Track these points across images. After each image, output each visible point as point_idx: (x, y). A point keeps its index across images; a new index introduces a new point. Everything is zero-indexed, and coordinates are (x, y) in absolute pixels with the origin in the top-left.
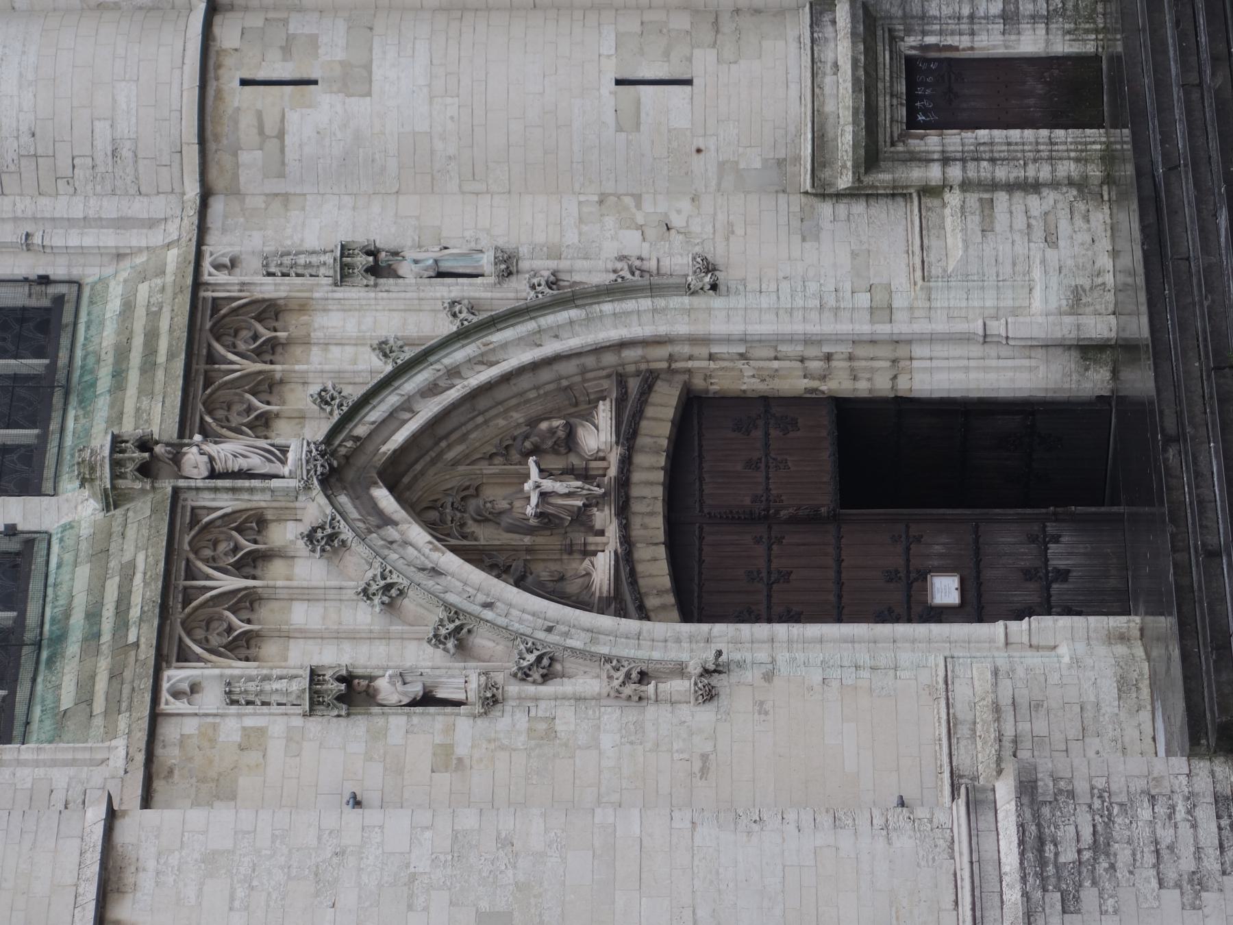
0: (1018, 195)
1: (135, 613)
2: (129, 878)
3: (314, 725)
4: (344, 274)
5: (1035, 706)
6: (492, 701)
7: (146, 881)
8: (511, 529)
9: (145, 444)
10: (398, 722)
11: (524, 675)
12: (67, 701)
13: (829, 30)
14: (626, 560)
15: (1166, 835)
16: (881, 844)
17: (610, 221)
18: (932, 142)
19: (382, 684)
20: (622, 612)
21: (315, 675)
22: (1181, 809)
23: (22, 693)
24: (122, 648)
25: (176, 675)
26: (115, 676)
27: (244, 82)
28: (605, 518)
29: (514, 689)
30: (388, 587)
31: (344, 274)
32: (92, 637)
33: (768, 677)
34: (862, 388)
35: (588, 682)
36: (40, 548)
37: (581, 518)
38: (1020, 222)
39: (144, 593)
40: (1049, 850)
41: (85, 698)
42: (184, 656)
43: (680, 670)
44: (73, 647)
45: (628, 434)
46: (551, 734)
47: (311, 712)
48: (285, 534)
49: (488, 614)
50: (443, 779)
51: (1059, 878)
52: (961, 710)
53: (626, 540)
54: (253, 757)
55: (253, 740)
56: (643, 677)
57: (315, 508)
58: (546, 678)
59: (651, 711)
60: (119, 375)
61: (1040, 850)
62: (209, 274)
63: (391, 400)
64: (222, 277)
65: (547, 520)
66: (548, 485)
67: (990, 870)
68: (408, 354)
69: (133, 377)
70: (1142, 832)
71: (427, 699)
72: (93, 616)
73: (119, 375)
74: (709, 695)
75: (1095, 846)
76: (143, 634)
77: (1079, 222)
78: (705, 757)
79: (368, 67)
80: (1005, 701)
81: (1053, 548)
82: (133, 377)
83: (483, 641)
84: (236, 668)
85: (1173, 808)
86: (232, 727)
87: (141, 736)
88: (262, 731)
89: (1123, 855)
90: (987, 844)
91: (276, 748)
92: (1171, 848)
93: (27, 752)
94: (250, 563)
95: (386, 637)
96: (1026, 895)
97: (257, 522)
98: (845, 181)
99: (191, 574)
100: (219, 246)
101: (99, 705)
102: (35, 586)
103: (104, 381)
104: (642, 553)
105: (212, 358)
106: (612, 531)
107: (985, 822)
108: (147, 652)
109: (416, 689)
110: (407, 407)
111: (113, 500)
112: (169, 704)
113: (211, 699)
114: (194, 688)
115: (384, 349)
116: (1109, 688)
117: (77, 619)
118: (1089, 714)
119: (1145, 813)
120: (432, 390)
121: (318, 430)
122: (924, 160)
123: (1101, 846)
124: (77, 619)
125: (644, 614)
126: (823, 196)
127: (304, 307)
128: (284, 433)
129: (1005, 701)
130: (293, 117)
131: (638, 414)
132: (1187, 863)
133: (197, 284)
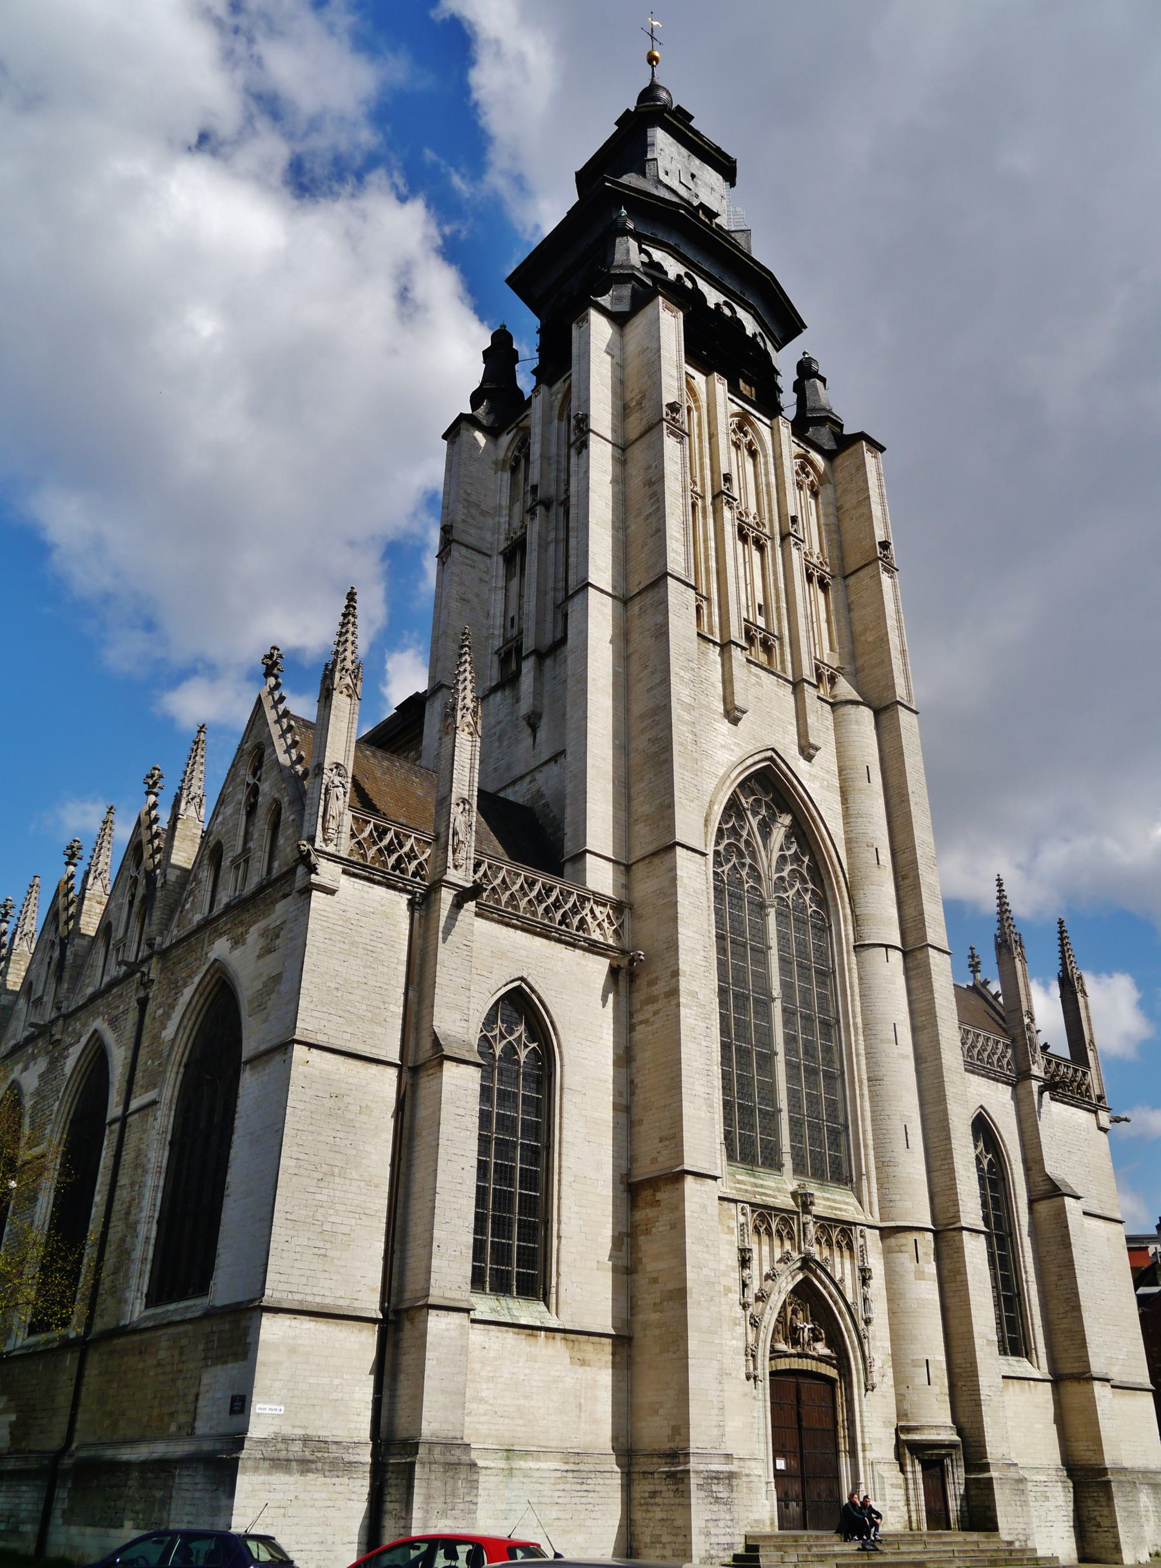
0: (905, 1498)
1: (764, 1198)
2: (699, 1182)
3: (736, 1250)
5: (750, 1489)
6: (745, 1306)
7: (698, 1187)
8: (791, 1319)
9: (812, 1203)
10: (737, 1276)
11: (752, 1317)
12: (738, 1177)
13: (950, 1433)
14: (787, 1355)
15: (721, 1524)
16: (714, 1423)
17: (883, 1357)
18: (919, 1468)
19: (747, 1271)
20: (771, 1352)
21: (750, 1250)
22: (728, 1530)
23: (738, 1165)
24: (755, 1193)
25: (748, 1208)
26: (746, 1191)
27: (916, 1240)
29: (748, 1313)
30: (774, 1275)
32: (756, 1185)
33: (754, 1398)
35: (751, 1338)
36: (778, 1173)
38: (896, 1498)
39: (770, 1201)
40: (715, 1481)
41: (739, 1182)
42: (753, 1211)
43: (755, 1368)
44: (753, 1180)
45: (821, 1359)
46: (736, 1324)
47: (739, 1249)
49: (768, 1307)
50: (722, 1289)
51: (707, 1484)
52: (748, 1463)
53: (791, 1356)
54: (726, 1230)
55: (730, 1231)
56: (753, 1356)
57: (796, 1255)
58: (751, 1324)
59: (744, 1358)
60: (828, 1199)
61: (715, 1478)
62: (859, 1228)
63: (828, 1282)
64: (858, 1232)
66: (806, 1330)
67: (708, 1461)
68: (841, 1288)
69: (828, 1203)
70: (722, 1515)
71: (745, 1285)
72: (762, 1186)
73: (828, 1199)
74: (748, 1378)
75: (717, 1498)
76: (758, 1200)
77: (897, 1519)
78: (730, 1374)
79: (923, 1279)
80: (752, 1478)
81: (795, 1504)
82: (828, 1203)
85: (729, 1527)
86: (733, 1224)
87: (730, 1196)
88: (733, 1233)
89: (715, 1508)
90: (716, 1460)
91: (728, 1237)
92: (717, 1525)
93: (725, 1163)
95: (761, 1274)
96: (702, 1472)
98: (903, 1437)
99: (776, 1216)
100: (868, 1231)
101: (737, 1185)
102: (768, 1171)
103: (826, 1195)
104: (787, 1360)
105: (836, 1227)
106: (793, 1351)
107: (722, 1460)
108: (753, 1200)
109: (748, 1282)
110: (825, 1287)
111: (794, 1195)
112: (740, 1205)
113: (742, 1219)
114: (744, 1214)
116: (756, 1516)
117: (761, 1182)
118: (749, 1508)
119: (728, 1517)
120: (831, 1296)
122: (913, 1465)
123: (717, 1500)
124: (761, 1182)
125: (771, 1359)
126: (896, 1430)
129: (752, 1478)
130: (906, 1255)
131: (827, 1363)
132: (713, 1531)
133: (855, 1224)
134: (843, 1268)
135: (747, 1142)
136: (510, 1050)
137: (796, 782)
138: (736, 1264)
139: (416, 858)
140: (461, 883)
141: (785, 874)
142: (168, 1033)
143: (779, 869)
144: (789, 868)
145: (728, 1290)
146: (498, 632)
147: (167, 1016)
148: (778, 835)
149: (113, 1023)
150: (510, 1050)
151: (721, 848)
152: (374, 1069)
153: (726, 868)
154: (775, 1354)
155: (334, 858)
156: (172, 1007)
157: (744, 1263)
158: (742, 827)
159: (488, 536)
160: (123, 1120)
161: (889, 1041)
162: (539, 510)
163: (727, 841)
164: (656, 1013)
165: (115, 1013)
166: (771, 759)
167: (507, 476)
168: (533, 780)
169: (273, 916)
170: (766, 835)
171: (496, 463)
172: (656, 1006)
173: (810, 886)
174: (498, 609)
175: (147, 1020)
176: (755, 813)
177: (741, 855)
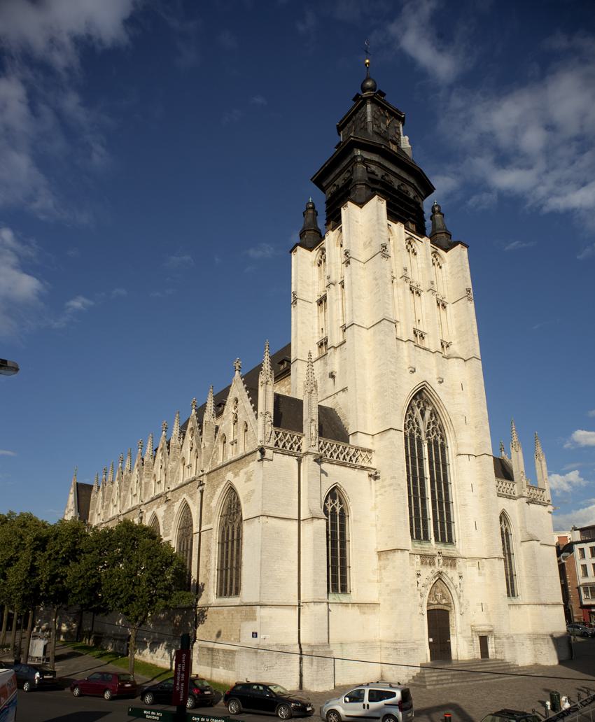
4: (459, 573)
14: (432, 604)
25: (419, 556)
28: (436, 602)
31: (459, 573)
34: (451, 631)
37: (436, 599)
44: (420, 546)
45: (445, 604)
48: (433, 568)
57: (436, 571)
65: (436, 596)
71: (418, 583)
76: (422, 553)
83: (424, 588)
84: (420, 564)
94: (430, 564)
97: (434, 564)
100: (461, 560)
115: (452, 578)
121: (444, 571)
127: (456, 569)
128: (443, 567)
134: (451, 574)
135: (418, 532)
136: (334, 509)
137: (434, 393)
138: (416, 576)
139: (297, 444)
140: (315, 452)
141: (430, 429)
142: (214, 504)
143: (428, 428)
144: (432, 426)
145: (412, 585)
146: (317, 335)
147: (212, 497)
148: (427, 414)
149: (191, 496)
150: (334, 509)
151: (407, 422)
152: (289, 522)
153: (409, 430)
154: (429, 604)
155: (270, 448)
156: (214, 494)
157: (419, 575)
158: (414, 413)
159: (311, 295)
160: (200, 533)
161: (469, 491)
162: (332, 286)
163: (408, 420)
164: (385, 492)
165: (191, 493)
166: (424, 385)
167: (317, 266)
168: (335, 398)
169: (250, 467)
170: (423, 415)
171: (312, 262)
172: (386, 489)
173: (440, 432)
174: (316, 326)
175: (204, 498)
176: (419, 407)
177: (413, 425)
